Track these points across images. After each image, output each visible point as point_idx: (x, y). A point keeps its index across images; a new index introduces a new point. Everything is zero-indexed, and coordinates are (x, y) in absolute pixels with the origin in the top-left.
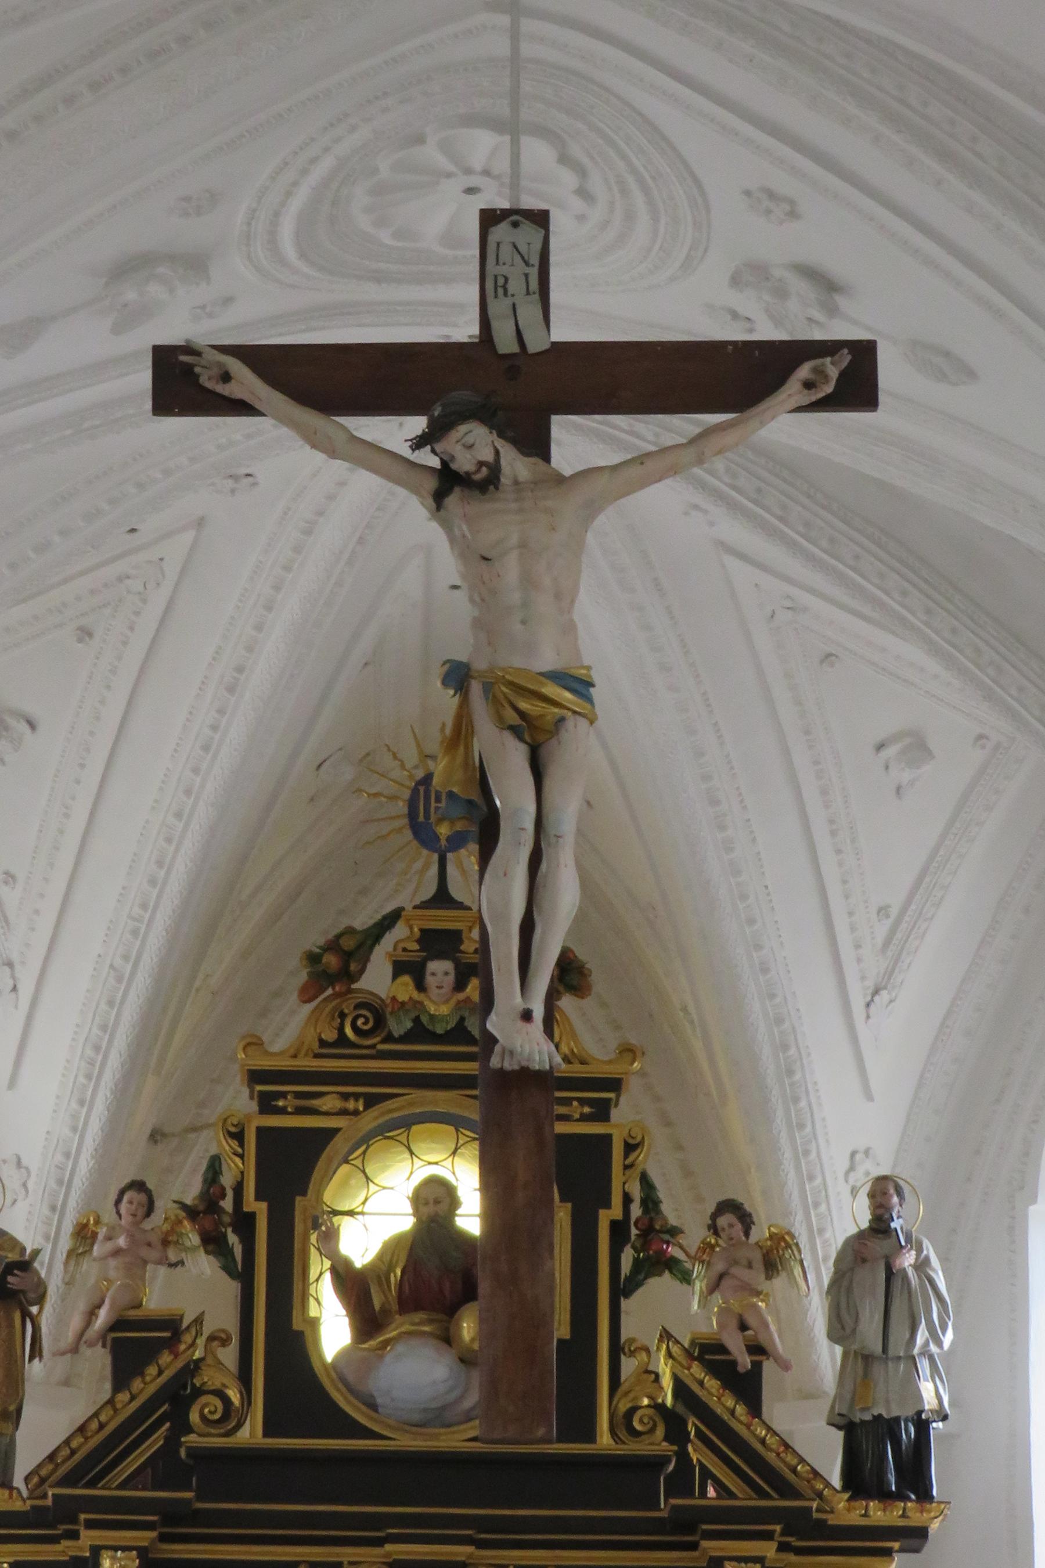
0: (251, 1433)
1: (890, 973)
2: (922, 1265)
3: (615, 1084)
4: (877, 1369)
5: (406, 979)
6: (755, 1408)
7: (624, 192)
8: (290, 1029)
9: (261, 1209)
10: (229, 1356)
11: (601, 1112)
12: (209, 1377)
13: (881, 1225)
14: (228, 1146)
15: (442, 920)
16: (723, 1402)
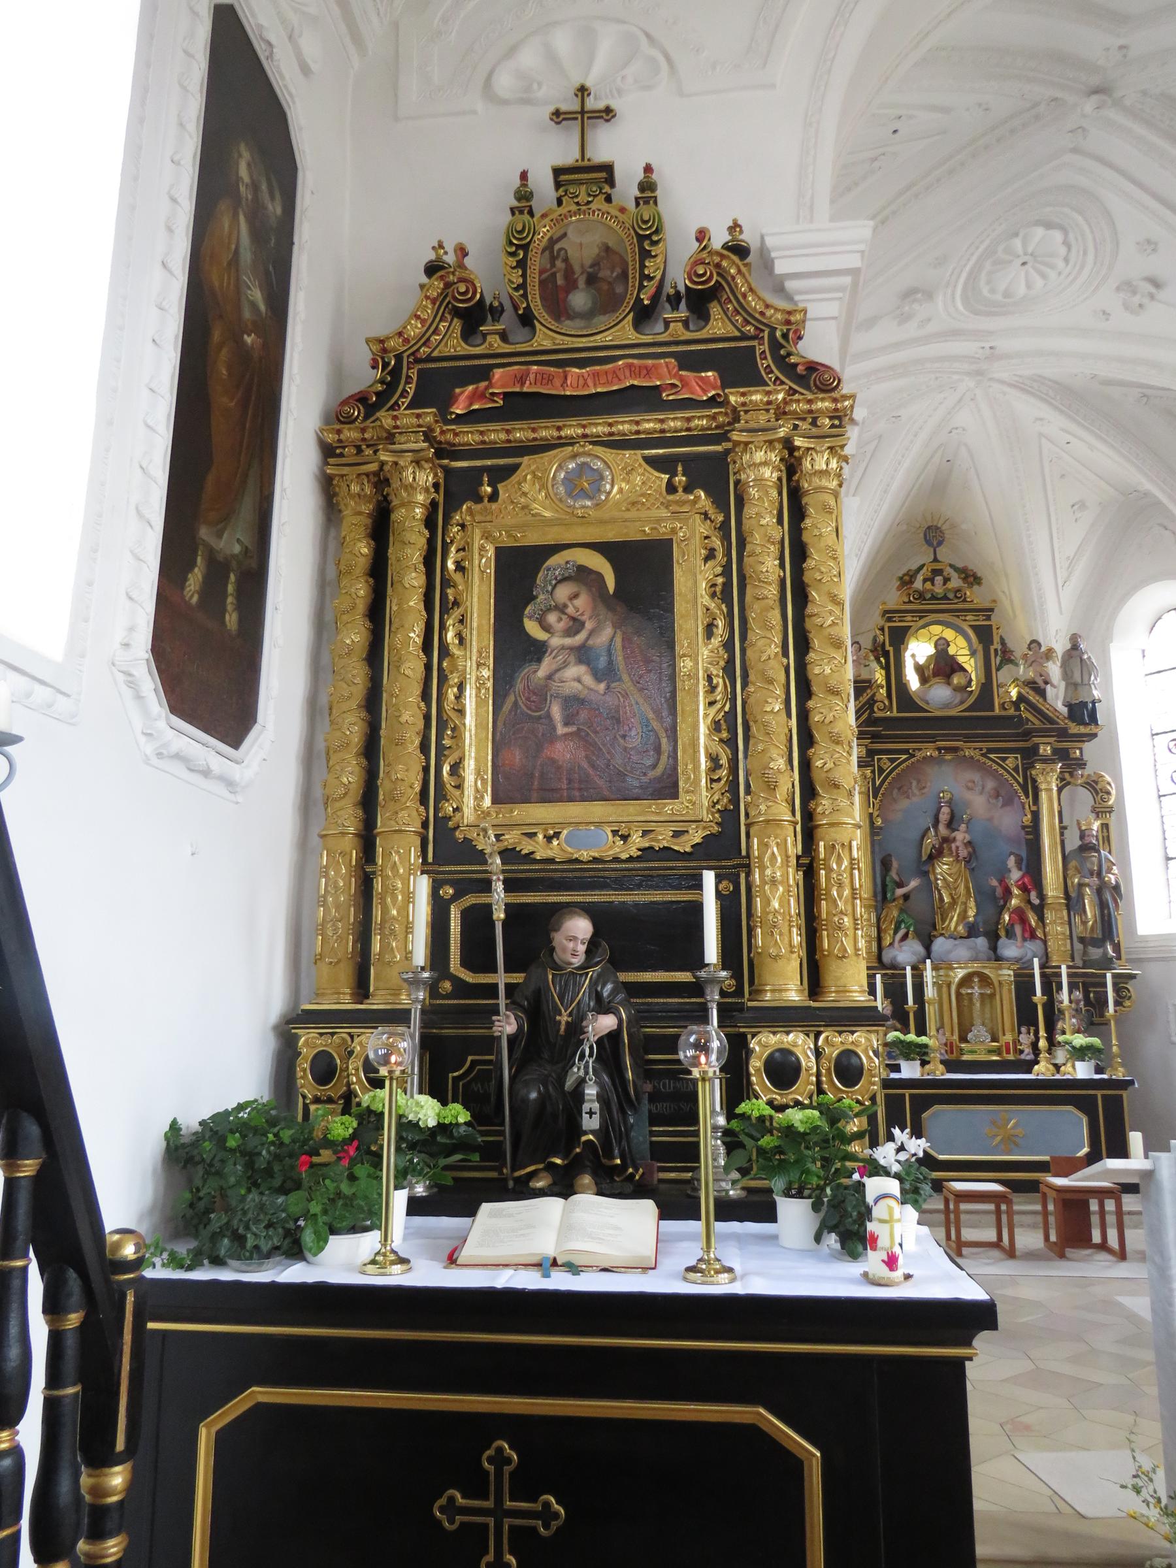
0: (895, 714)
1: (1069, 577)
2: (1089, 658)
3: (992, 610)
4: (1079, 688)
5: (929, 583)
6: (1045, 699)
7: (1085, 253)
8: (894, 598)
9: (891, 649)
10: (883, 691)
11: (989, 618)
12: (878, 697)
13: (1075, 647)
14: (878, 632)
15: (937, 566)
16: (1032, 697)
